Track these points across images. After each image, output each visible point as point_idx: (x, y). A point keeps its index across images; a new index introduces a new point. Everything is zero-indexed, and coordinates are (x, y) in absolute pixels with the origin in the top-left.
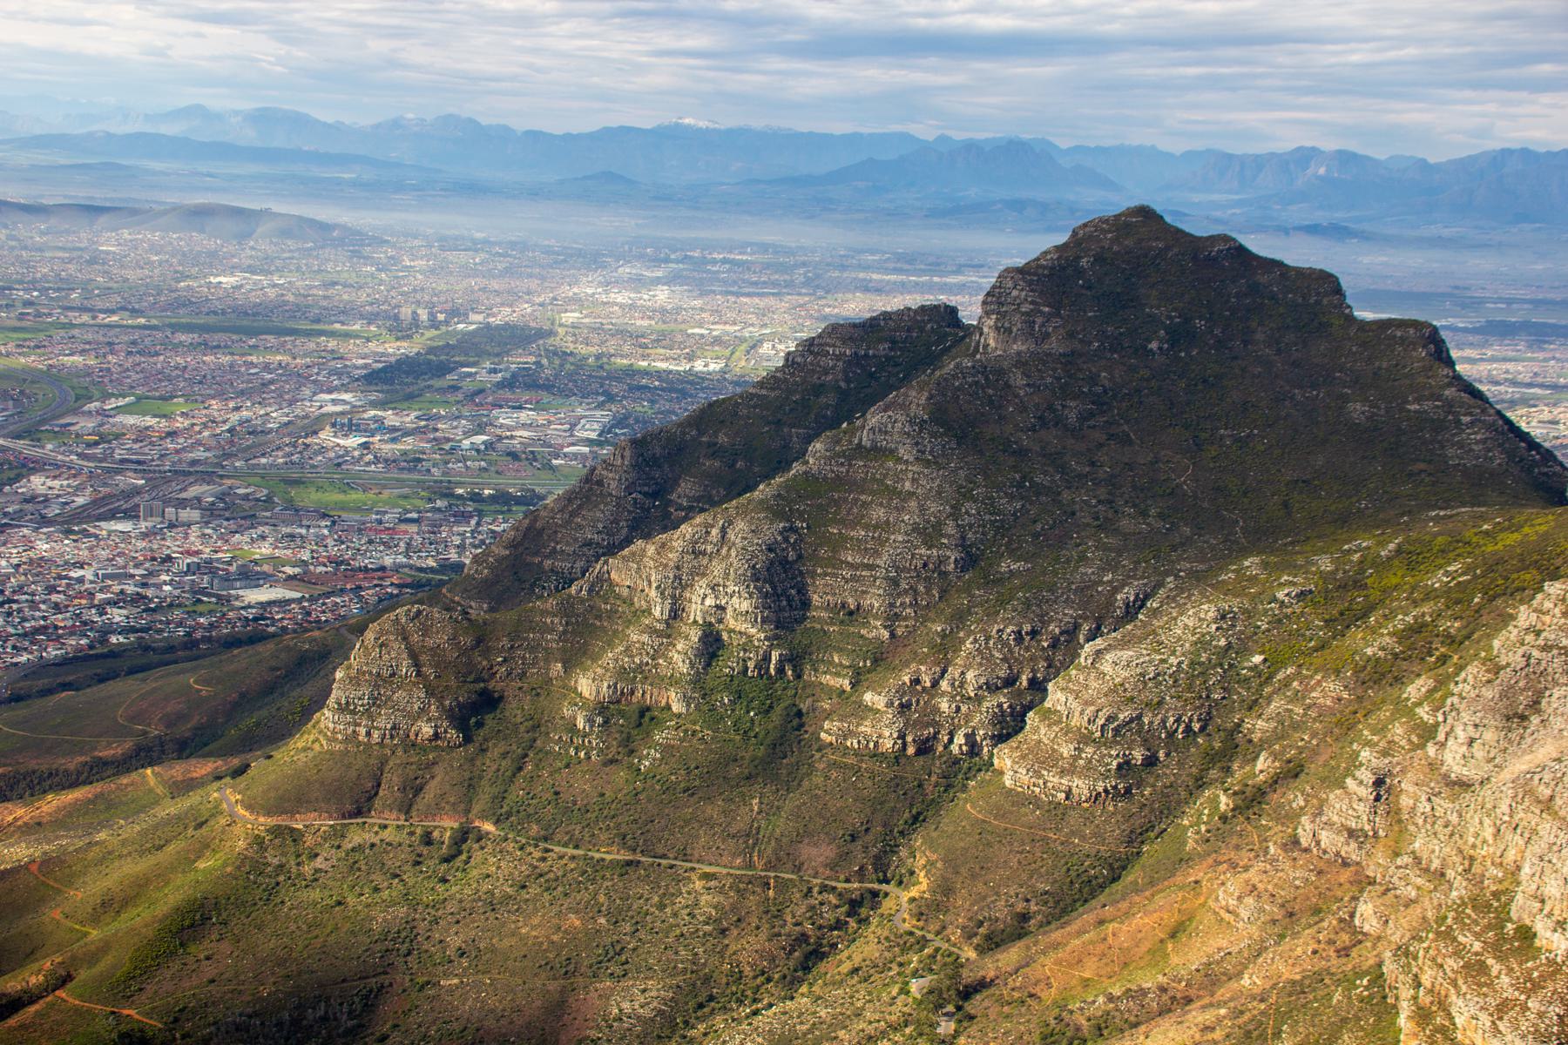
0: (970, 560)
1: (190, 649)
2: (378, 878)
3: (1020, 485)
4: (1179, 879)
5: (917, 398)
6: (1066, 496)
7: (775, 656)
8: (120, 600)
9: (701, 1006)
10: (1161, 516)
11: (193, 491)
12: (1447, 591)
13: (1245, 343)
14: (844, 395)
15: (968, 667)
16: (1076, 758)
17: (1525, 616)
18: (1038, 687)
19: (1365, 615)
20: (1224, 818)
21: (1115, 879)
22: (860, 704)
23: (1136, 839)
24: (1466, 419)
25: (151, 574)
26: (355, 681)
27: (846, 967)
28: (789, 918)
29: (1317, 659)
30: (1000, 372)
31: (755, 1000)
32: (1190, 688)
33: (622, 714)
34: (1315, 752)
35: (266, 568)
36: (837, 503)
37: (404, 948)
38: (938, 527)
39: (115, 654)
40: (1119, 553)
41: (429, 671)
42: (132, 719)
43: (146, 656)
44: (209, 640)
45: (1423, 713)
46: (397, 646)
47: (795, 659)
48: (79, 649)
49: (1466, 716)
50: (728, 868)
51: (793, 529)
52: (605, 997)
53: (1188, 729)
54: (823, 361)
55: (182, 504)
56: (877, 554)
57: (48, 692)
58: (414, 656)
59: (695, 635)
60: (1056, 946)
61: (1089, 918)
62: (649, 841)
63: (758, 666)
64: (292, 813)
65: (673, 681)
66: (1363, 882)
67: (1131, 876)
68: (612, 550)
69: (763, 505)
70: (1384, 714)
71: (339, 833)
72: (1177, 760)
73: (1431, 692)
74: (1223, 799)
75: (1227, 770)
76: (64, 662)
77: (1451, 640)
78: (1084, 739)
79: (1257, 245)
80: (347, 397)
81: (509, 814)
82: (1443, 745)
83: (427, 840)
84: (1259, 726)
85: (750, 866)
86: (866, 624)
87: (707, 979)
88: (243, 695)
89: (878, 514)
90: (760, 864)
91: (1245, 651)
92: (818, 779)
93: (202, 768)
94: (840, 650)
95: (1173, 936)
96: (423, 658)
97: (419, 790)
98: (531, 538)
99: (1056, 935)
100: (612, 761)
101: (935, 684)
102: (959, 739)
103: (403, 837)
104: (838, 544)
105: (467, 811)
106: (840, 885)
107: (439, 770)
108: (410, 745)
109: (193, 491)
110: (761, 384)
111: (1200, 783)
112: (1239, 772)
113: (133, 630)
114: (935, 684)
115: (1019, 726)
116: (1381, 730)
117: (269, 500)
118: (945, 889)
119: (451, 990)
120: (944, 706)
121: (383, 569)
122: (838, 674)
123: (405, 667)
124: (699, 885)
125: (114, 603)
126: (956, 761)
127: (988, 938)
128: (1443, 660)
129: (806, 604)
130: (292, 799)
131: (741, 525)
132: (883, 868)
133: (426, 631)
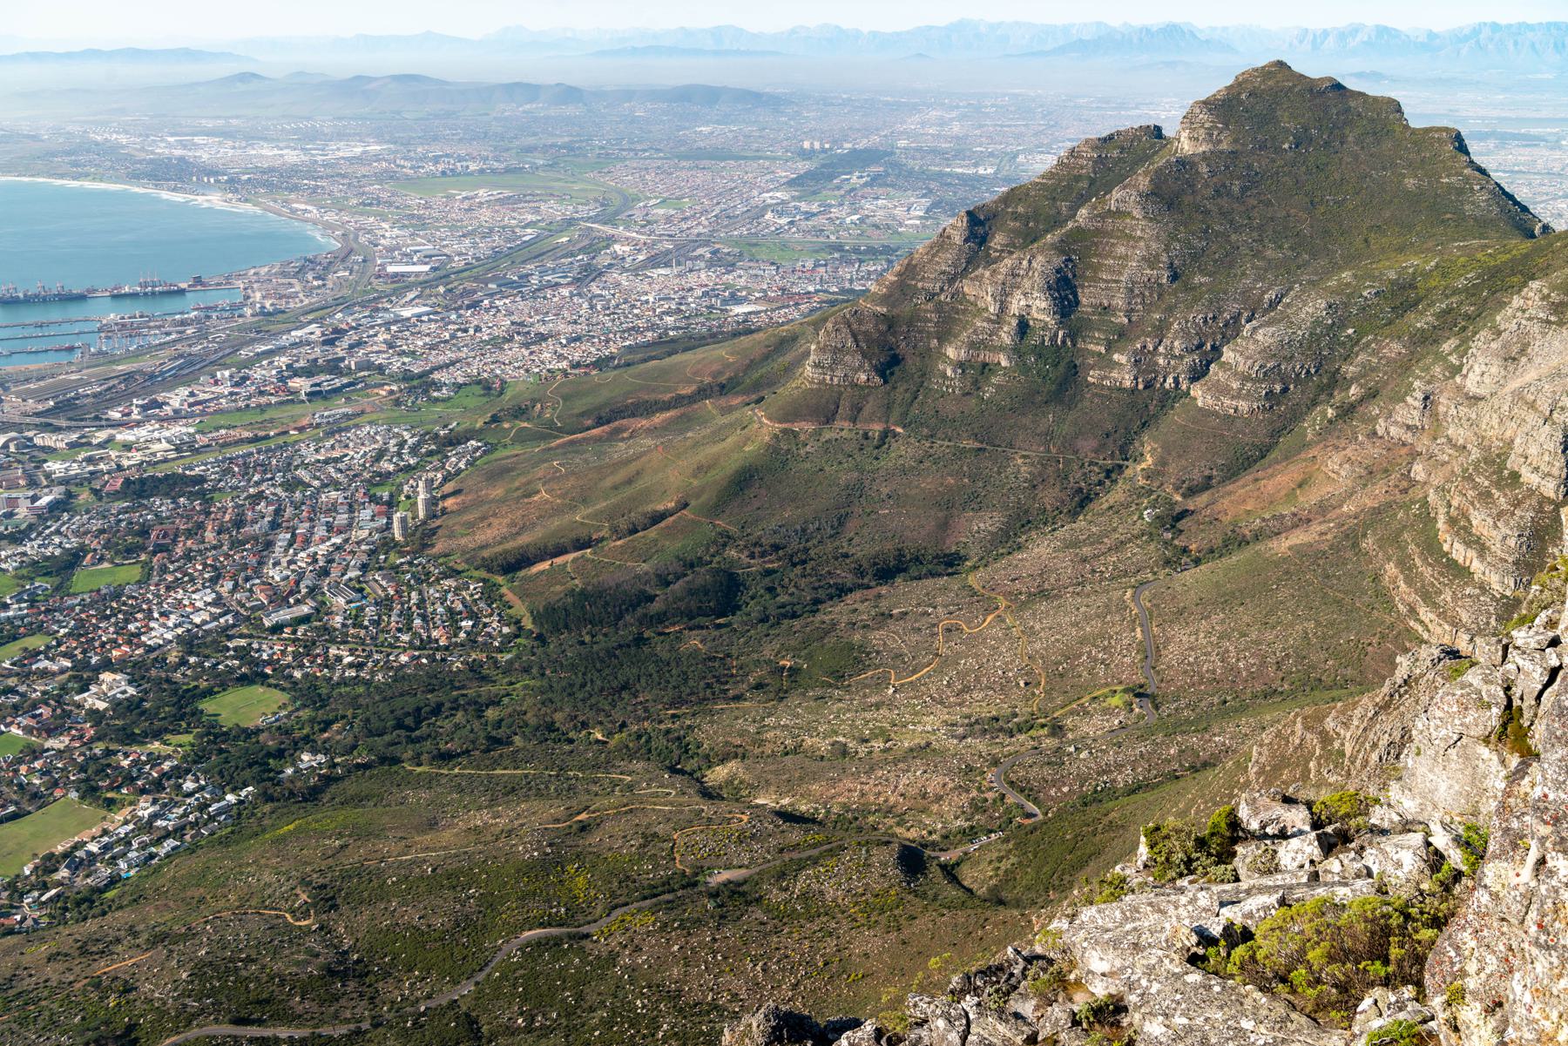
0: (1174, 277)
1: (713, 337)
2: (840, 457)
3: (1206, 232)
4: (1303, 456)
5: (1143, 182)
6: (1234, 237)
7: (1061, 334)
8: (667, 313)
10: (1292, 249)
11: (700, 251)
12: (1466, 289)
13: (1342, 143)
14: (1092, 182)
15: (1175, 339)
16: (1241, 389)
17: (1517, 301)
18: (1216, 350)
19: (1416, 304)
20: (1330, 421)
21: (1263, 457)
23: (1276, 434)
24: (1477, 187)
27: (1105, 506)
29: (1387, 331)
30: (1193, 165)
32: (1310, 348)
33: (972, 367)
34: (1386, 383)
36: (1096, 244)
38: (1157, 256)
39: (673, 341)
40: (1266, 270)
41: (864, 345)
42: (695, 374)
43: (690, 342)
45: (1453, 359)
46: (845, 330)
47: (1073, 335)
49: (1481, 359)
50: (1037, 451)
51: (1070, 260)
52: (970, 520)
53: (1308, 372)
54: (1081, 161)
56: (1120, 273)
58: (854, 336)
59: (1014, 322)
60: (1230, 493)
61: (1250, 478)
62: (991, 437)
63: (1051, 339)
64: (792, 422)
65: (1002, 349)
66: (1414, 455)
67: (1272, 456)
68: (964, 273)
69: (1053, 246)
70: (1429, 360)
71: (818, 433)
72: (1307, 388)
73: (1457, 347)
74: (1330, 411)
75: (1331, 395)
76: (649, 345)
77: (1468, 317)
78: (1246, 378)
79: (1351, 84)
80: (778, 194)
82: (1465, 376)
84: (1351, 370)
86: (1114, 315)
87: (1027, 511)
89: (1121, 250)
90: (1054, 451)
91: (1344, 327)
92: (1087, 404)
93: (737, 401)
95: (1300, 486)
98: (910, 270)
99: (1230, 488)
101: (1156, 348)
102: (1170, 380)
103: (852, 435)
104: (1096, 268)
107: (871, 399)
108: (855, 385)
109: (700, 251)
110: (1043, 177)
111: (1314, 403)
112: (1338, 396)
114: (1156, 348)
115: (1205, 372)
116: (1427, 369)
117: (741, 254)
118: (1162, 462)
119: (885, 516)
120: (1161, 361)
123: (850, 343)
124: (1020, 461)
125: (667, 313)
126: (1168, 392)
127: (1189, 489)
128: (1464, 329)
129: (1078, 303)
130: (791, 413)
131: (1040, 258)
132: (1126, 452)
133: (860, 322)
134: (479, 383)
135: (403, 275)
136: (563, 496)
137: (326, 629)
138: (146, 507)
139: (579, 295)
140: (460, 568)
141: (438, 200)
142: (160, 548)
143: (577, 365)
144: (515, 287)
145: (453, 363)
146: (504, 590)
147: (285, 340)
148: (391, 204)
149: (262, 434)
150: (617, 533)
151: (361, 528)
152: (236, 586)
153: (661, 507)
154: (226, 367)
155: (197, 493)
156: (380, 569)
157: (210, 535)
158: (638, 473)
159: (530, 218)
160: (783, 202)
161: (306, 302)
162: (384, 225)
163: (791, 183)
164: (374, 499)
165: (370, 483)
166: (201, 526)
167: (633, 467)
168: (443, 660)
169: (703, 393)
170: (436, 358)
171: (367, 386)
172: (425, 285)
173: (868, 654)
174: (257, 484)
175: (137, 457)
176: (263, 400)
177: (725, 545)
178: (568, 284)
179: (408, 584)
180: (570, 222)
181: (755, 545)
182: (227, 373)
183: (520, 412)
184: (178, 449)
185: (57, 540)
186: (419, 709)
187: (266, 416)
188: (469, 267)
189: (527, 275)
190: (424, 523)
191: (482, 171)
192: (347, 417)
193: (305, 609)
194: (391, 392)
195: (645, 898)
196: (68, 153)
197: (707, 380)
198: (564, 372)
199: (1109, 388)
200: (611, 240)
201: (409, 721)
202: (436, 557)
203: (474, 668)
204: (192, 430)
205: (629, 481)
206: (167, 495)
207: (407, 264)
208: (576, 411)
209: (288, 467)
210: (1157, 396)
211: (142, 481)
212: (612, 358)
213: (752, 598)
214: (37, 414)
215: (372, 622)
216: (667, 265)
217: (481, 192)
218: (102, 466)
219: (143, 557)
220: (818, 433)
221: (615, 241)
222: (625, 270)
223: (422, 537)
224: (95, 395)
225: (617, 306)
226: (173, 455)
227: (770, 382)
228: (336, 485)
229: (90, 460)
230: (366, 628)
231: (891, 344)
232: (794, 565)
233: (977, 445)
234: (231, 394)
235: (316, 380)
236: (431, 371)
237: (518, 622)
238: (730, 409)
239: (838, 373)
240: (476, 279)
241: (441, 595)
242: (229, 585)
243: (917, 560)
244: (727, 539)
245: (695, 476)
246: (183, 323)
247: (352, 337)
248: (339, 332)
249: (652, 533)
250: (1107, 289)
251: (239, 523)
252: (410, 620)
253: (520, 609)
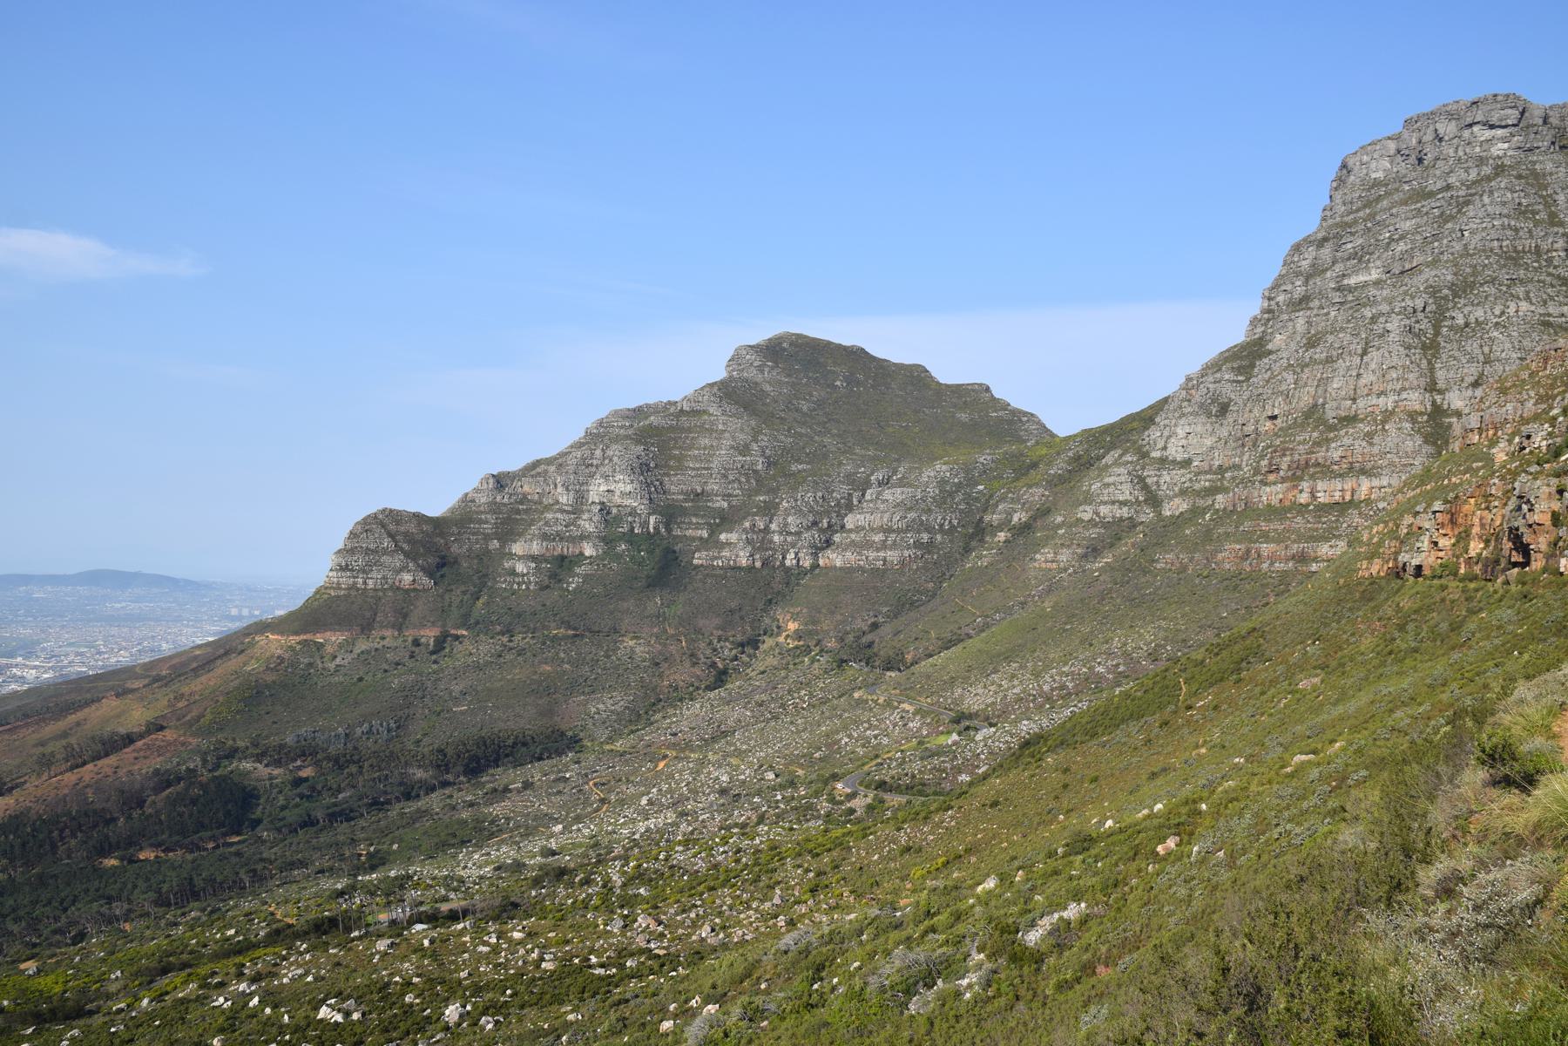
7: (652, 519)
33: (547, 561)
41: (406, 547)
65: (583, 537)
81: (477, 623)
83: (416, 643)
89: (706, 441)
97: (405, 616)
100: (547, 587)
102: (791, 556)
123: (387, 543)
199: (721, 568)
210: (779, 575)
220: (348, 646)
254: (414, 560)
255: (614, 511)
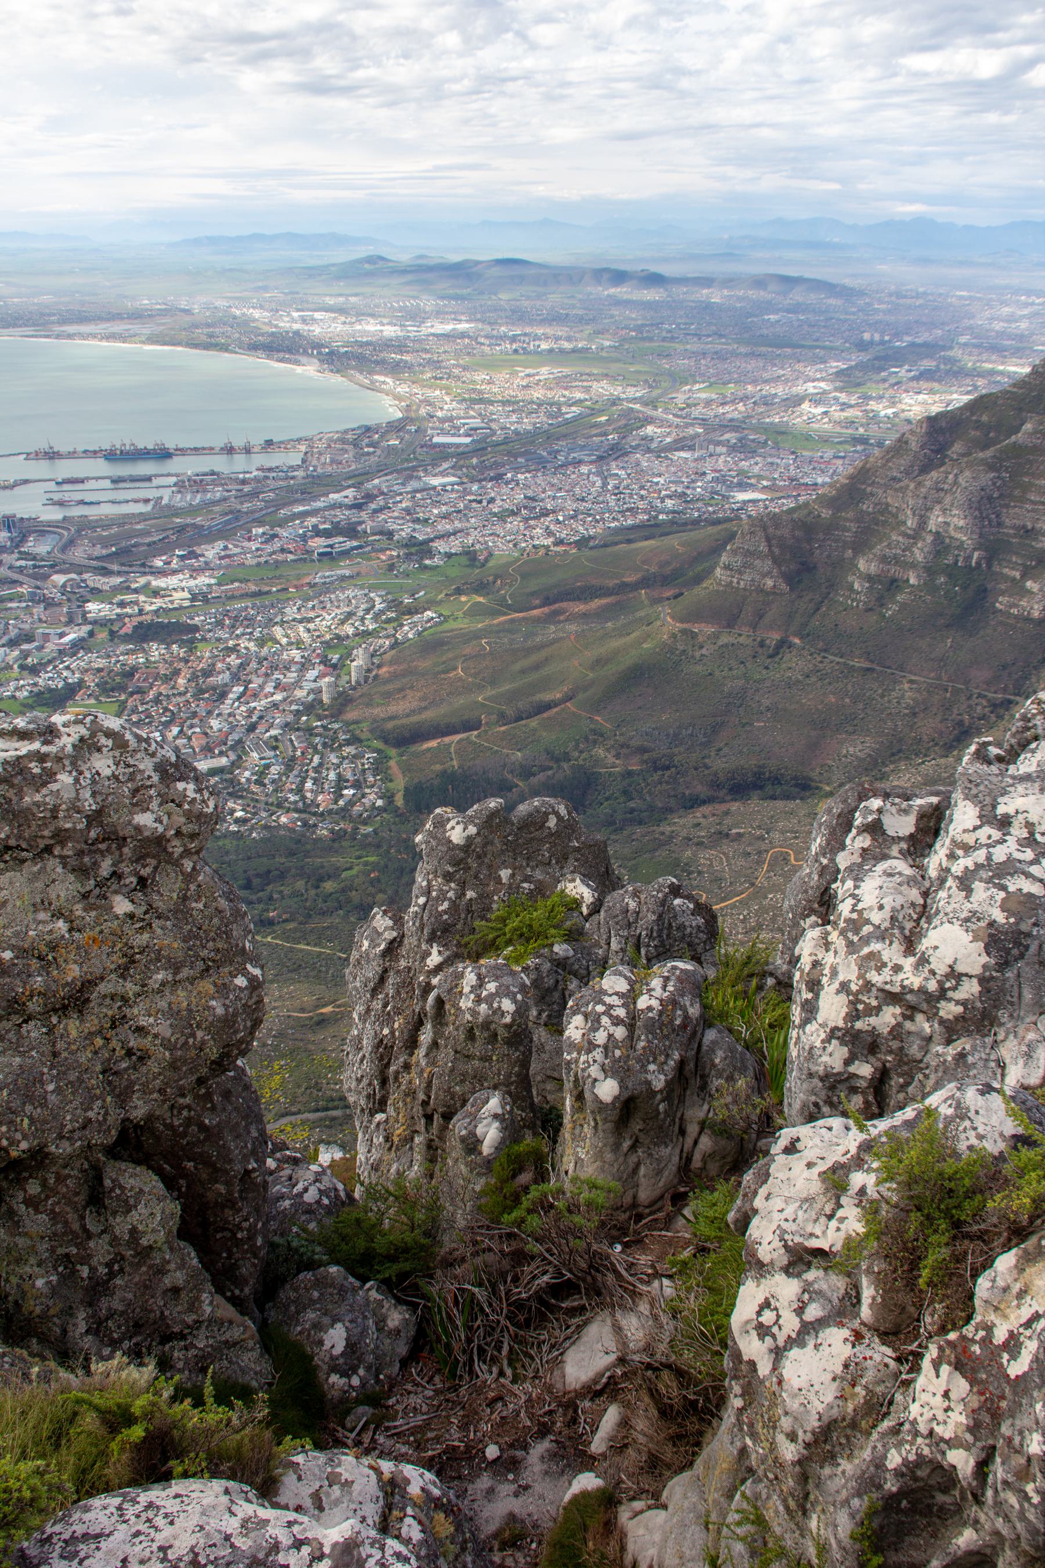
2: (733, 663)
7: (976, 555)
9: (893, 755)
11: (727, 436)
22: (1023, 588)
25: (693, 481)
26: (734, 552)
28: (956, 711)
31: (925, 756)
33: (880, 582)
35: (753, 481)
37: (738, 703)
41: (776, 551)
42: (644, 562)
44: (706, 520)
46: (760, 534)
48: (641, 521)
55: (719, 443)
57: (616, 544)
58: (768, 540)
59: (929, 539)
65: (913, 566)
69: (983, 462)
76: (633, 528)
80: (822, 385)
81: (808, 635)
83: (762, 644)
85: (939, 678)
87: (900, 740)
88: (699, 554)
90: (945, 677)
94: (1017, 554)
96: (773, 542)
97: (761, 617)
100: (871, 610)
103: (749, 641)
104: (1026, 488)
105: (787, 631)
106: (990, 695)
108: (761, 590)
109: (727, 436)
110: (1014, 385)
113: (674, 512)
117: (765, 443)
119: (759, 729)
121: (816, 484)
122: (1013, 569)
123: (763, 547)
124: (906, 686)
125: (670, 497)
134: (467, 553)
135: (444, 445)
136: (475, 675)
137: (233, 782)
138: (144, 650)
139: (598, 474)
140: (363, 736)
141: (501, 376)
142: (140, 691)
143: (559, 542)
144: (541, 465)
145: (454, 534)
146: (392, 763)
147: (319, 504)
148: (458, 378)
149: (267, 589)
150: (503, 718)
151: (301, 688)
152: (181, 731)
153: (547, 697)
154: (261, 523)
155: (187, 641)
156: (298, 729)
157: (181, 681)
158: (547, 660)
159: (579, 395)
160: (824, 392)
161: (353, 467)
162: (447, 399)
163: (840, 373)
164: (325, 661)
165: (327, 645)
166: (177, 673)
167: (544, 653)
168: (315, 826)
169: (646, 582)
170: (444, 526)
171: (374, 550)
172: (461, 454)
173: (690, 873)
174: (238, 637)
175: (159, 603)
176: (281, 557)
177: (595, 742)
178: (591, 462)
179: (315, 748)
180: (615, 401)
181: (622, 746)
182: (261, 530)
183: (481, 587)
184: (194, 598)
185: (65, 673)
186: (269, 872)
187: (278, 573)
188: (506, 441)
189: (558, 452)
190: (354, 689)
191: (551, 351)
192: (343, 578)
193: (224, 761)
194: (391, 557)
195: (317, 1110)
196: (208, 326)
197: (653, 569)
198: (547, 547)
199: (1016, 617)
200: (649, 420)
201: (256, 881)
202: (347, 724)
203: (337, 837)
204: (213, 581)
205: (537, 667)
206: (162, 641)
207: (453, 435)
208: (528, 590)
209: (270, 623)
211: (151, 625)
212: (591, 538)
213: (607, 799)
214: (97, 559)
215: (273, 782)
216: (691, 448)
217: (544, 370)
218: (128, 610)
219: (123, 697)
220: (716, 636)
221: (650, 423)
222: (649, 450)
223: (343, 700)
224: (149, 545)
225: (627, 487)
226: (187, 603)
227: (698, 580)
228: (299, 644)
229: (122, 604)
230: (265, 785)
231: (805, 549)
232: (656, 769)
233: (867, 665)
234: (258, 550)
235: (330, 542)
236: (432, 540)
237: (393, 796)
238: (658, 601)
239: (746, 577)
240: (509, 453)
241: (337, 765)
242: (175, 730)
243: (776, 780)
244: (597, 736)
245: (592, 668)
246: (244, 482)
247: (380, 501)
248: (370, 497)
249: (534, 723)
250: (1033, 511)
251: (208, 673)
252: (303, 782)
253: (400, 783)
254: (779, 566)
255: (947, 541)
